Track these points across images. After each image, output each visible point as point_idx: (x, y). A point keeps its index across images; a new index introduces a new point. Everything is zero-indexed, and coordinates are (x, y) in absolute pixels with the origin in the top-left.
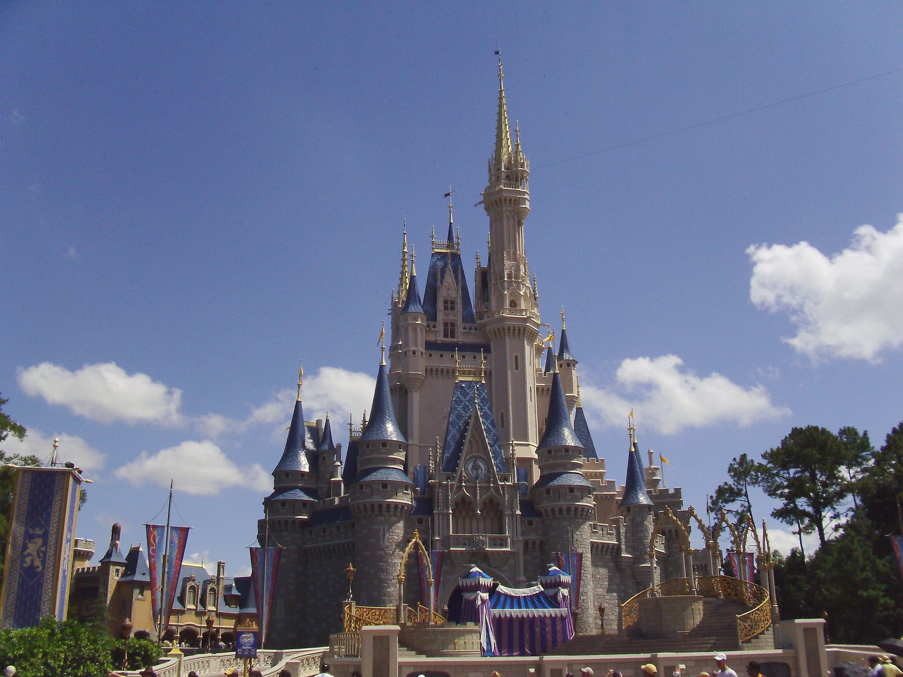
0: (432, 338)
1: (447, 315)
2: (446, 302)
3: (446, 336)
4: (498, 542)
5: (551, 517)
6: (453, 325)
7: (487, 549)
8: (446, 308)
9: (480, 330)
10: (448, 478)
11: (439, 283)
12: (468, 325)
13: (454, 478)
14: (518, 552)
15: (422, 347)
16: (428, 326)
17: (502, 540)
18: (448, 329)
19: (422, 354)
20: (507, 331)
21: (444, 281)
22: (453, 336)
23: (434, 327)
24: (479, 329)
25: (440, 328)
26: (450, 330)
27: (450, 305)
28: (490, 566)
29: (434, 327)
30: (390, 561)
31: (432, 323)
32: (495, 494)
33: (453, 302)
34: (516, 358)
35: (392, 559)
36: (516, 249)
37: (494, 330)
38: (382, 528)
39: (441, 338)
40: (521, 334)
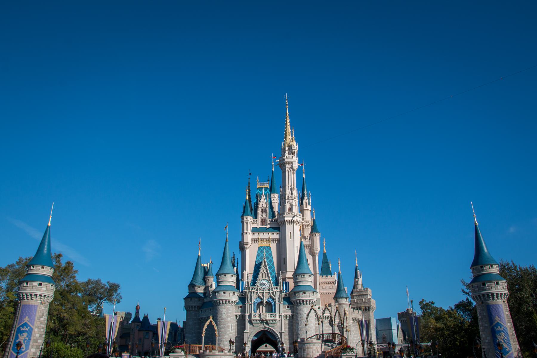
0: (255, 226)
1: (262, 216)
2: (262, 209)
3: (262, 224)
4: (272, 316)
5: (296, 304)
6: (265, 219)
7: (267, 319)
8: (262, 212)
9: (276, 221)
10: (252, 289)
11: (259, 202)
13: (254, 288)
14: (281, 320)
15: (250, 231)
16: (254, 221)
17: (274, 315)
18: (262, 222)
19: (250, 233)
20: (286, 222)
23: (256, 221)
24: (276, 221)
25: (259, 221)
26: (264, 221)
28: (268, 325)
29: (256, 221)
30: (226, 324)
31: (255, 220)
32: (272, 295)
33: (265, 210)
34: (291, 233)
35: (227, 323)
36: (291, 185)
37: (281, 222)
38: (223, 310)
39: (259, 226)
40: (293, 223)
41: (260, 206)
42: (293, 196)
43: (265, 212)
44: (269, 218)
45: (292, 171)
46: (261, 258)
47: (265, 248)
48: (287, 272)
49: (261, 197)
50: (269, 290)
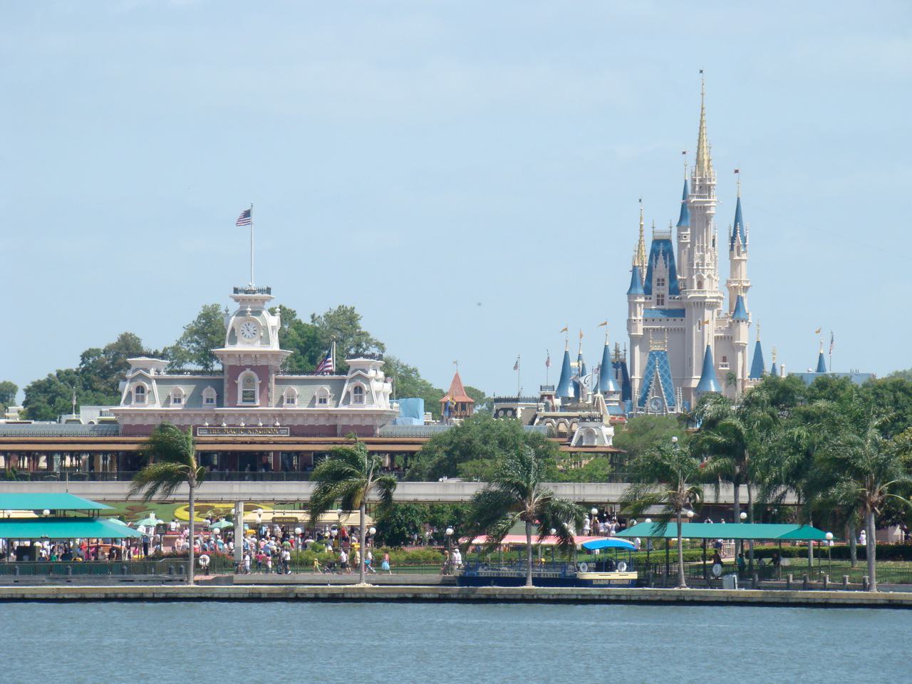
1: (658, 289)
2: (659, 280)
3: (658, 304)
6: (663, 296)
8: (658, 285)
10: (640, 410)
11: (654, 267)
12: (672, 296)
16: (646, 298)
21: (657, 266)
22: (662, 304)
23: (650, 299)
26: (660, 301)
27: (661, 282)
31: (648, 296)
33: (663, 280)
41: (656, 276)
42: (706, 262)
43: (663, 284)
44: (670, 294)
45: (705, 220)
46: (654, 368)
47: (658, 353)
48: (693, 380)
49: (657, 259)
50: (663, 412)
